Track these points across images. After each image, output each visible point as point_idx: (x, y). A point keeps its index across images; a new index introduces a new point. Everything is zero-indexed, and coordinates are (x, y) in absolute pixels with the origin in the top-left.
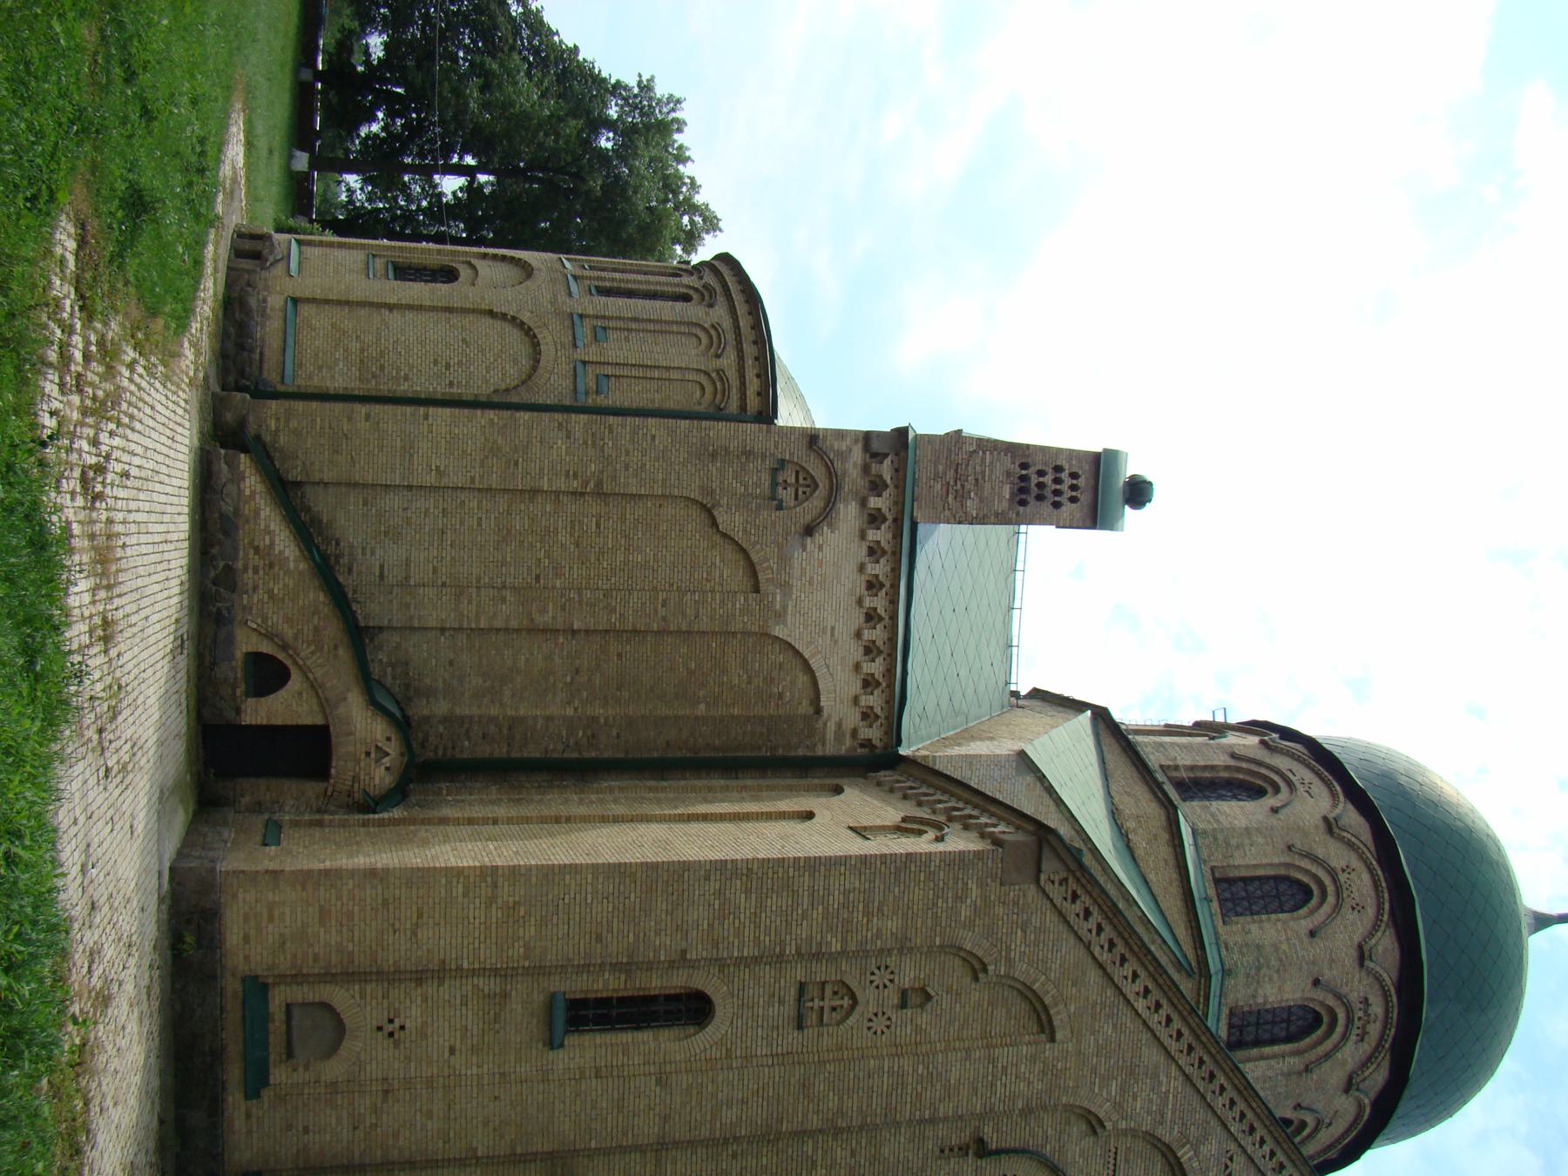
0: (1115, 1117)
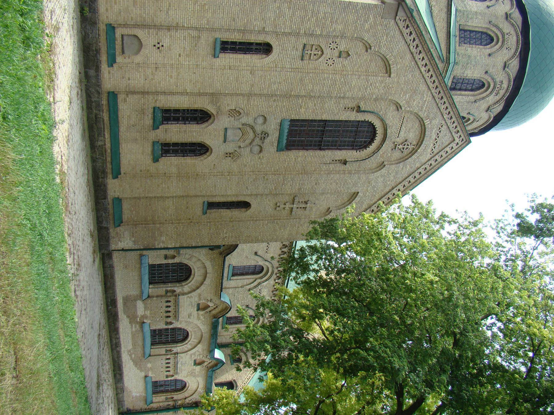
0: (406, 106)
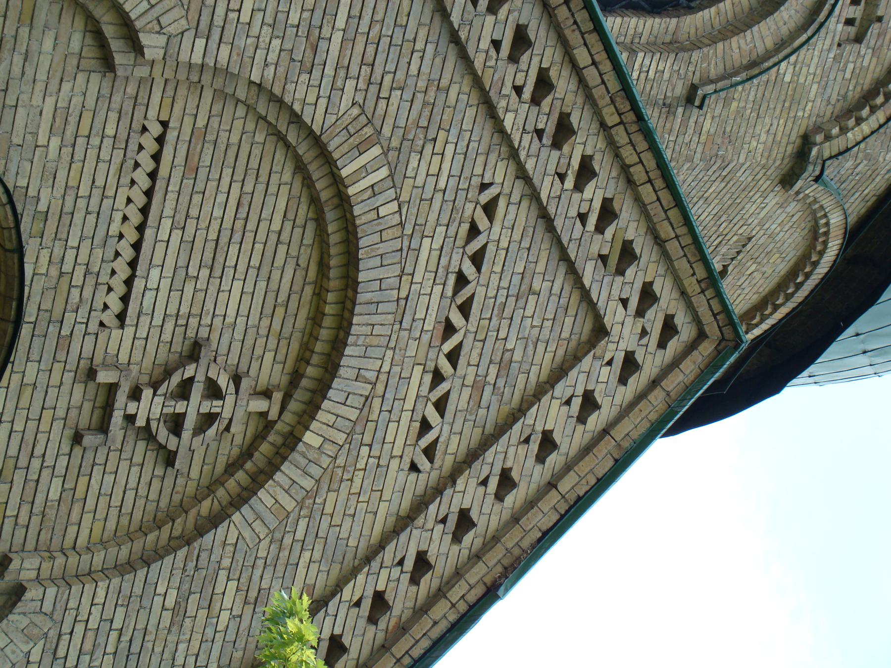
0: (175, 22)
